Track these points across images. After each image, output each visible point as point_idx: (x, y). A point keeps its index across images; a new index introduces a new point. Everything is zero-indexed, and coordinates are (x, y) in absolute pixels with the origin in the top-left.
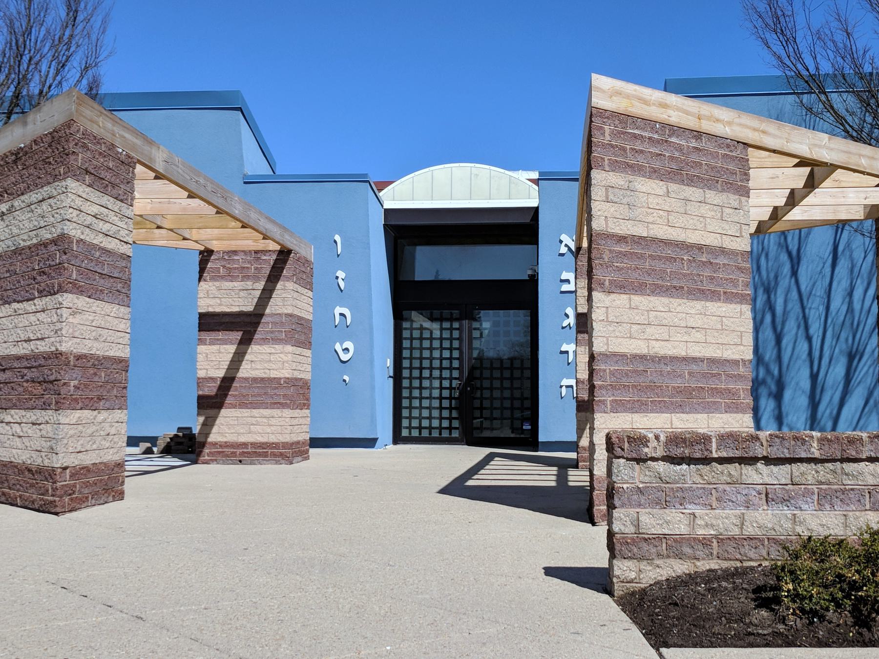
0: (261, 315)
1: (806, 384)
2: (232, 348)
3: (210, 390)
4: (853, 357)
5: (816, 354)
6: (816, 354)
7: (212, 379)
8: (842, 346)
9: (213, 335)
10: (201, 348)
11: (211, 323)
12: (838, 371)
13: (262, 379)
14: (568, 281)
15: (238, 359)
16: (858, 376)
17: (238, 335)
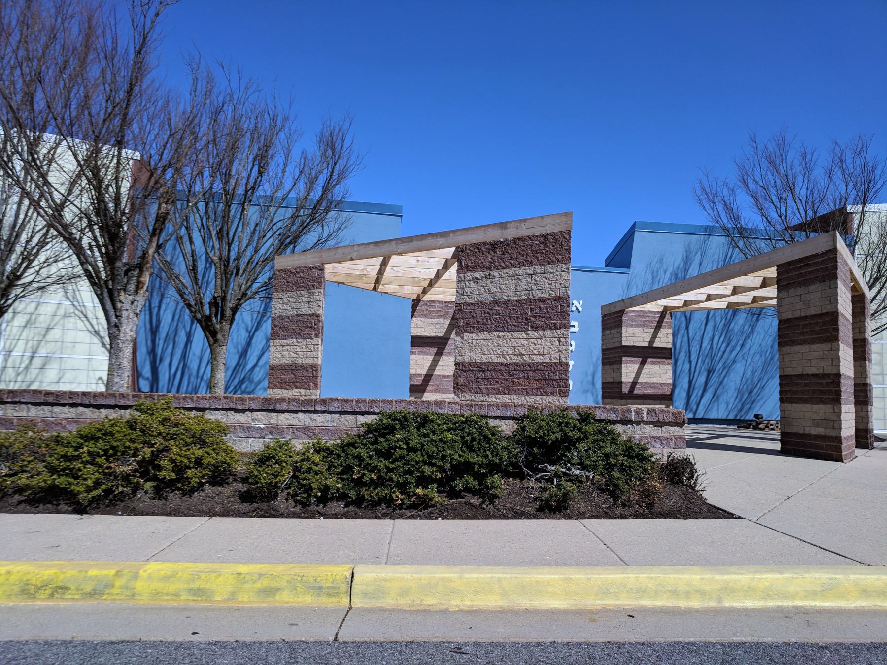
0: (448, 339)
1: (686, 386)
2: (431, 358)
3: (418, 381)
4: (710, 372)
5: (693, 370)
6: (693, 370)
7: (420, 375)
8: (706, 366)
9: (420, 349)
10: (413, 357)
11: (418, 342)
12: (702, 379)
14: (574, 326)
15: (434, 363)
17: (434, 350)
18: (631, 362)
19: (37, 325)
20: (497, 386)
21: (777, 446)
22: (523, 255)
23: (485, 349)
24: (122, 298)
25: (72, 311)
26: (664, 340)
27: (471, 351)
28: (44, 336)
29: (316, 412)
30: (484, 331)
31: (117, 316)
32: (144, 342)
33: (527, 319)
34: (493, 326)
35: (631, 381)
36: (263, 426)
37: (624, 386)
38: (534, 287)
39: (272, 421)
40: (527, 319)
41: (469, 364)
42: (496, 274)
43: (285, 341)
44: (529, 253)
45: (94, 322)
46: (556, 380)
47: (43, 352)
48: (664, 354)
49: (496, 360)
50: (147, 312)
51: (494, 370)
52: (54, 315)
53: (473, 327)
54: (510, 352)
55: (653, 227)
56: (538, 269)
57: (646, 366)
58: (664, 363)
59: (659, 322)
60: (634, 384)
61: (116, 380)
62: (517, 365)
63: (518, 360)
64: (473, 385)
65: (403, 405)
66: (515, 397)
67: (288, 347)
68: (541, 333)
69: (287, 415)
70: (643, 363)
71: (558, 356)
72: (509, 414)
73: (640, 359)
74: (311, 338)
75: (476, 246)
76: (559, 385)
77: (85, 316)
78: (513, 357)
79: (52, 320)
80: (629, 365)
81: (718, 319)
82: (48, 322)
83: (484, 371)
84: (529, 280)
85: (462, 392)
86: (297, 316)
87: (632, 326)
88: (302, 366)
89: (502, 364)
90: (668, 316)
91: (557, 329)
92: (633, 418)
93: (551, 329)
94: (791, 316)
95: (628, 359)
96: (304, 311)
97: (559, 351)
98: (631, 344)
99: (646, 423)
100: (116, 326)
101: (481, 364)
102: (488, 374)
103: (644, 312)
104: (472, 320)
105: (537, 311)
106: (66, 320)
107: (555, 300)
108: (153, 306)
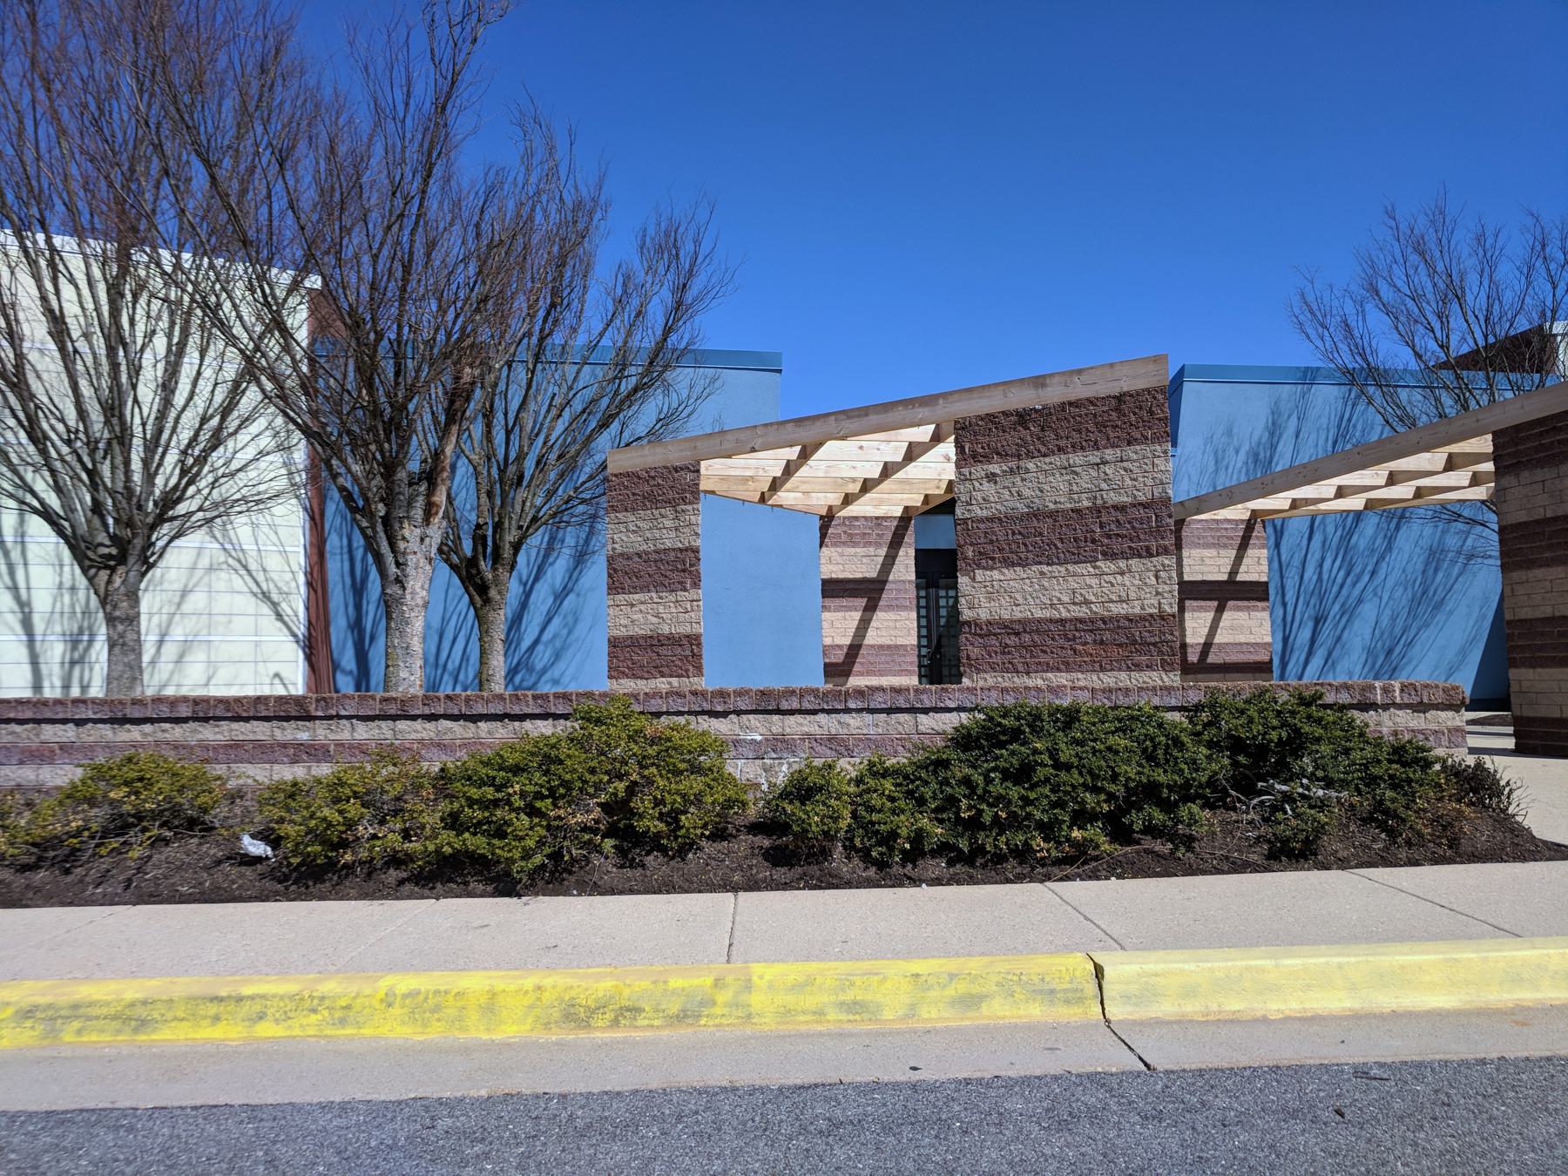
2: (857, 615)
3: (838, 657)
4: (1318, 621)
5: (1289, 618)
6: (1289, 618)
7: (840, 647)
8: (1311, 611)
10: (826, 615)
11: (834, 589)
12: (1305, 634)
13: (889, 647)
15: (864, 625)
16: (1321, 639)
17: (862, 602)
18: (1200, 609)
19: (166, 586)
20: (1043, 658)
21: (1510, 743)
22: (1080, 432)
23: (1018, 596)
24: (406, 533)
25: (222, 559)
26: (1256, 567)
27: (990, 599)
28: (179, 605)
29: (847, 711)
30: (1013, 565)
31: (398, 564)
32: (342, 609)
33: (1093, 541)
34: (1030, 556)
35: (1202, 641)
36: (759, 738)
37: (1189, 650)
38: (1104, 486)
39: (774, 730)
40: (1093, 541)
41: (989, 623)
42: (1031, 466)
43: (637, 596)
44: (1091, 427)
45: (260, 577)
46: (1154, 644)
47: (177, 633)
48: (1255, 592)
49: (1039, 614)
50: (346, 557)
51: (1037, 631)
52: (193, 568)
53: (993, 559)
54: (1066, 599)
55: (1214, 374)
56: (1109, 454)
57: (1226, 615)
58: (1255, 609)
59: (1243, 537)
60: (1207, 646)
61: (403, 674)
62: (1081, 621)
63: (1081, 612)
64: (998, 659)
65: (994, 694)
66: (1080, 675)
67: (643, 607)
68: (1122, 564)
69: (799, 718)
70: (1220, 610)
71: (1155, 603)
72: (1173, 702)
73: (1216, 603)
74: (685, 590)
75: (990, 418)
76: (1161, 653)
77: (245, 567)
78: (1072, 608)
79: (191, 576)
80: (1196, 614)
81: (1330, 529)
82: (184, 580)
83: (1017, 634)
84: (1094, 474)
85: (979, 671)
86: (657, 552)
87: (1198, 546)
88: (670, 637)
89: (1051, 620)
90: (1258, 527)
91: (1151, 555)
92: (1379, 699)
93: (1140, 556)
94: (1525, 519)
95: (1195, 603)
96: (668, 544)
97: (1158, 593)
98: (1199, 578)
99: (1400, 707)
100: (398, 581)
101: (1012, 622)
102: (1027, 638)
103: (1217, 521)
104: (989, 547)
105: (1113, 526)
106: (214, 576)
107: (1144, 506)
108: (355, 545)
